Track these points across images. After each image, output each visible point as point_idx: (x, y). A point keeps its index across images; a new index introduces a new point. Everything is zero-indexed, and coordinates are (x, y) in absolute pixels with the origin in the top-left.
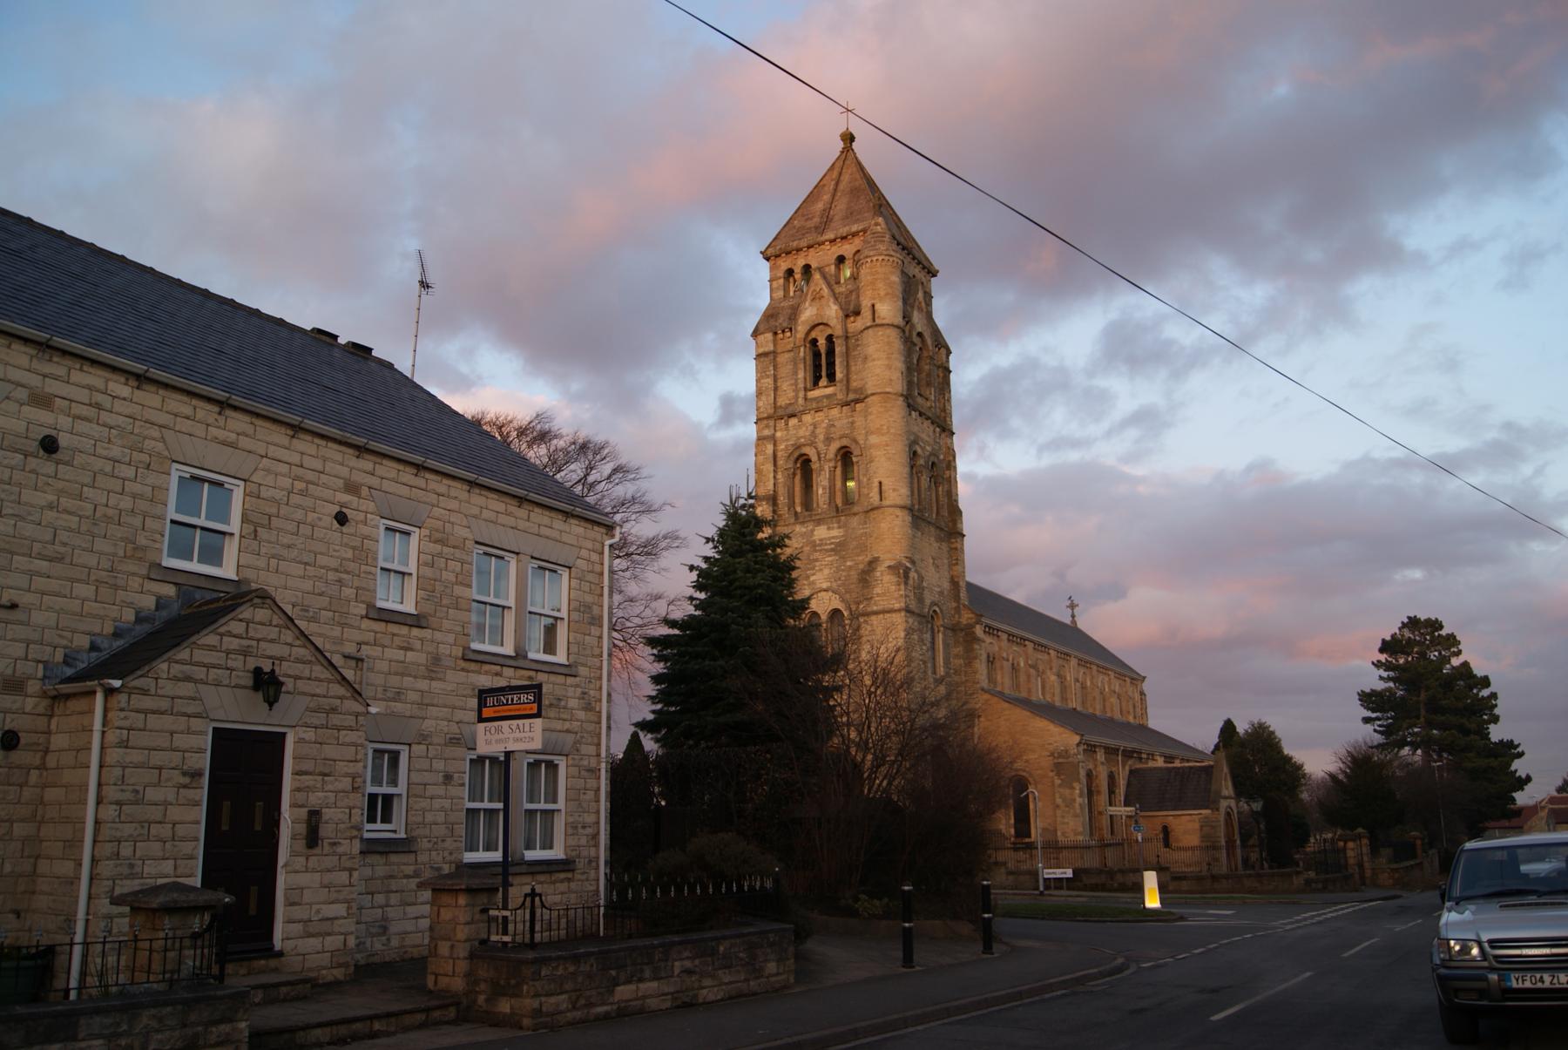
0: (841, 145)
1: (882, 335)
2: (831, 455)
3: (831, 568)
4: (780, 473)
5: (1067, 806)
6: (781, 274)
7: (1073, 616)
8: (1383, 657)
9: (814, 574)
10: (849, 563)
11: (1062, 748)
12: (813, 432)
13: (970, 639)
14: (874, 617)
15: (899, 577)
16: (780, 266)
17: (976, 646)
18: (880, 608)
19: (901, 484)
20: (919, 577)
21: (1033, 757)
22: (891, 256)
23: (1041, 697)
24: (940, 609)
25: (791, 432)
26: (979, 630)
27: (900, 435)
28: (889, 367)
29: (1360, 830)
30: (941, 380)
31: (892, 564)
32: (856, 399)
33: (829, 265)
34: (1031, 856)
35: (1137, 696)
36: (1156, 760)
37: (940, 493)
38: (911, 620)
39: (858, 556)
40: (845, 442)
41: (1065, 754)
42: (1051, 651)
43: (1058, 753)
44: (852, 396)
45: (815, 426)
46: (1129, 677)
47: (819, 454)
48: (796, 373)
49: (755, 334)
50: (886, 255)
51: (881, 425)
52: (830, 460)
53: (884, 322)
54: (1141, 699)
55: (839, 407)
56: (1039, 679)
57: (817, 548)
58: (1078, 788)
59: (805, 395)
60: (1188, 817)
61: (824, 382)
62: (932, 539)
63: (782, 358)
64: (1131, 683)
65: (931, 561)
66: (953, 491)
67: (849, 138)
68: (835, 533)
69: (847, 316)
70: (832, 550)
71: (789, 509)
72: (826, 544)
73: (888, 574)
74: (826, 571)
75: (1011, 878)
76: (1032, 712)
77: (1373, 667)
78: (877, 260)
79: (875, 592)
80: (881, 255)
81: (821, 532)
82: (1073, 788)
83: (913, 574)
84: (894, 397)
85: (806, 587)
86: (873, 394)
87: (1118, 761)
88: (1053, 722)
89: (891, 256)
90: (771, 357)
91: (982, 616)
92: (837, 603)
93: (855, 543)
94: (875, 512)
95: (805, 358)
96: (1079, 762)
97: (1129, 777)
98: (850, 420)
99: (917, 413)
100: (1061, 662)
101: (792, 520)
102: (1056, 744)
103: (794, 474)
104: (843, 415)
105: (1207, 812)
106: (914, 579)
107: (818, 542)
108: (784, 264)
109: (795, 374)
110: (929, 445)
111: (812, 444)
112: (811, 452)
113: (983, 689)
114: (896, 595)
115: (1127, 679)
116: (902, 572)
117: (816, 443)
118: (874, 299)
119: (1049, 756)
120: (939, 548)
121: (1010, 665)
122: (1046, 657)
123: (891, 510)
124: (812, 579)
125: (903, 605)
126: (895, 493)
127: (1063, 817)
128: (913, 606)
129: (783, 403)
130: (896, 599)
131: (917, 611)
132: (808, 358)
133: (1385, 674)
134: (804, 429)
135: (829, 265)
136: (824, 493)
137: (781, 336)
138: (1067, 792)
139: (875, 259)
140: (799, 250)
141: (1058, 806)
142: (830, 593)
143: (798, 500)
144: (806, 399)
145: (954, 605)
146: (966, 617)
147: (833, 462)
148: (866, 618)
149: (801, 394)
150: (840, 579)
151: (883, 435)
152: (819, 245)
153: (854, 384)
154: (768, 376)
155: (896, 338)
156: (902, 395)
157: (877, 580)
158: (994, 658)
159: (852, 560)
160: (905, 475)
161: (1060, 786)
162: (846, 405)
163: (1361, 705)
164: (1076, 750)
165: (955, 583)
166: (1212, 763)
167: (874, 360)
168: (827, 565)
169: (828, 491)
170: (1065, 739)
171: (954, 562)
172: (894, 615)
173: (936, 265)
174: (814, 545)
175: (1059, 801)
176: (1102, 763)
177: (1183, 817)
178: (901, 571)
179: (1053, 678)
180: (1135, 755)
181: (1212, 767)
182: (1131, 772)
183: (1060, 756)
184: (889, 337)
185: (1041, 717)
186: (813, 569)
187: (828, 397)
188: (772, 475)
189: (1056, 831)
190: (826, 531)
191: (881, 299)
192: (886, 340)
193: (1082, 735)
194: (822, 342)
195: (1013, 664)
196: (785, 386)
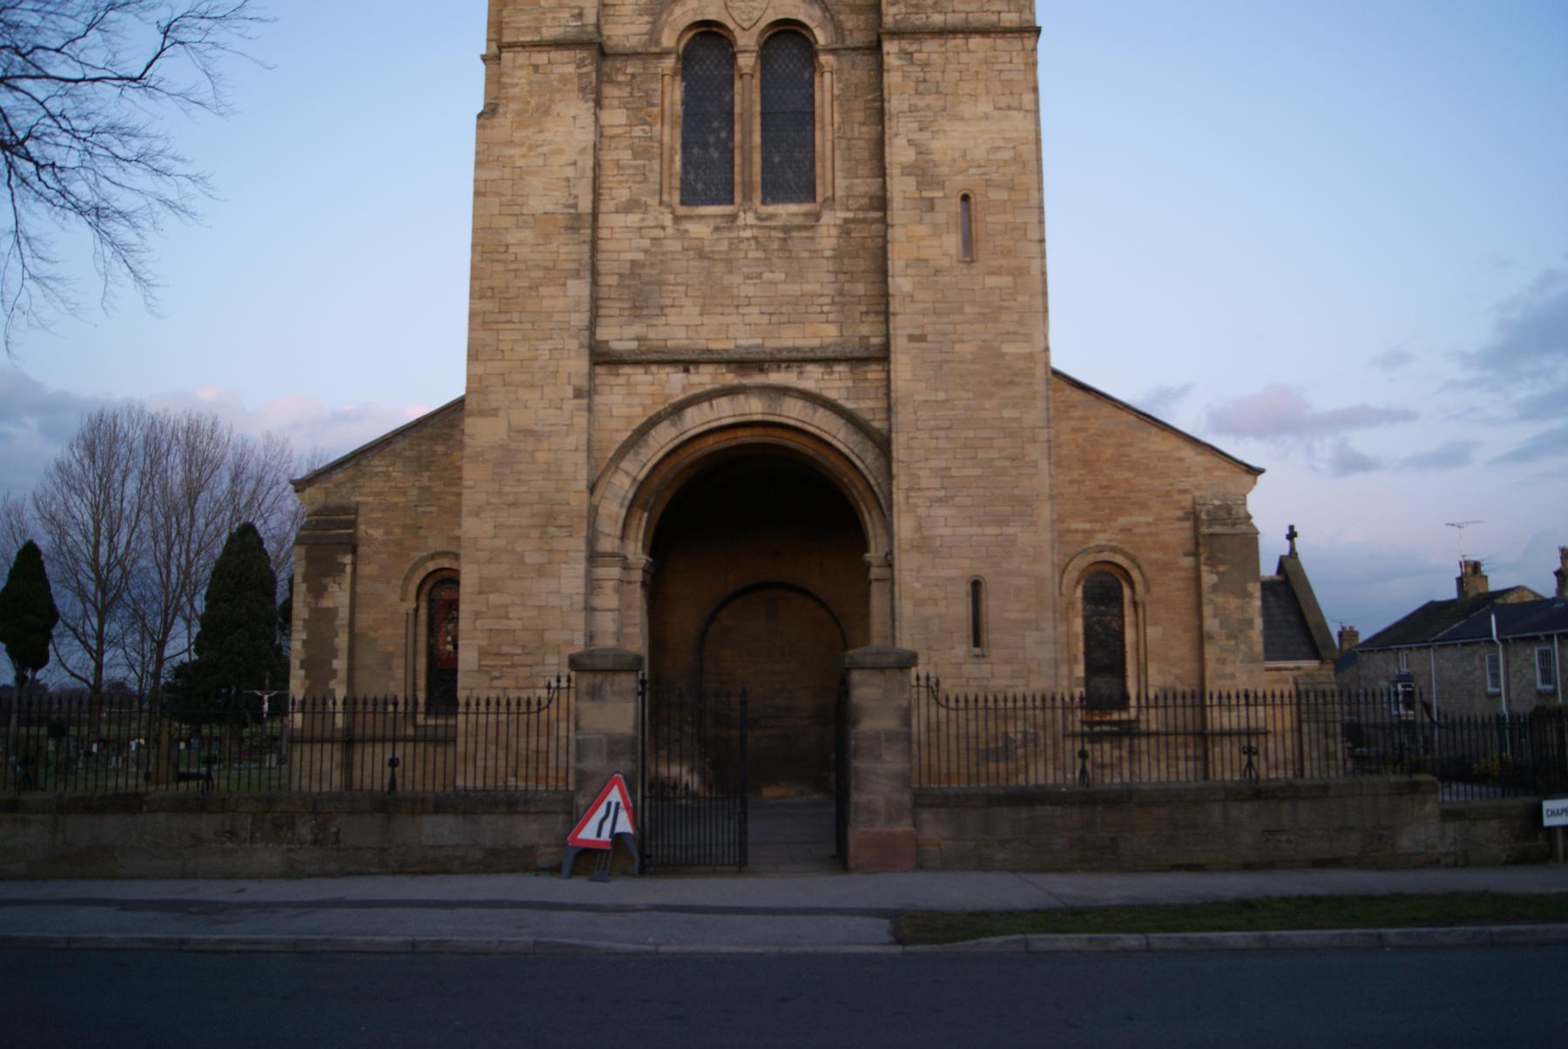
5: (1231, 636)
11: (1217, 503)
14: (932, 46)
18: (954, 19)
21: (1143, 519)
34: (1131, 752)
43: (1208, 512)
75: (1451, 829)
82: (1247, 595)
119: (1180, 519)
127: (1222, 661)
138: (1233, 602)
172: (1000, 43)
183: (1214, 520)
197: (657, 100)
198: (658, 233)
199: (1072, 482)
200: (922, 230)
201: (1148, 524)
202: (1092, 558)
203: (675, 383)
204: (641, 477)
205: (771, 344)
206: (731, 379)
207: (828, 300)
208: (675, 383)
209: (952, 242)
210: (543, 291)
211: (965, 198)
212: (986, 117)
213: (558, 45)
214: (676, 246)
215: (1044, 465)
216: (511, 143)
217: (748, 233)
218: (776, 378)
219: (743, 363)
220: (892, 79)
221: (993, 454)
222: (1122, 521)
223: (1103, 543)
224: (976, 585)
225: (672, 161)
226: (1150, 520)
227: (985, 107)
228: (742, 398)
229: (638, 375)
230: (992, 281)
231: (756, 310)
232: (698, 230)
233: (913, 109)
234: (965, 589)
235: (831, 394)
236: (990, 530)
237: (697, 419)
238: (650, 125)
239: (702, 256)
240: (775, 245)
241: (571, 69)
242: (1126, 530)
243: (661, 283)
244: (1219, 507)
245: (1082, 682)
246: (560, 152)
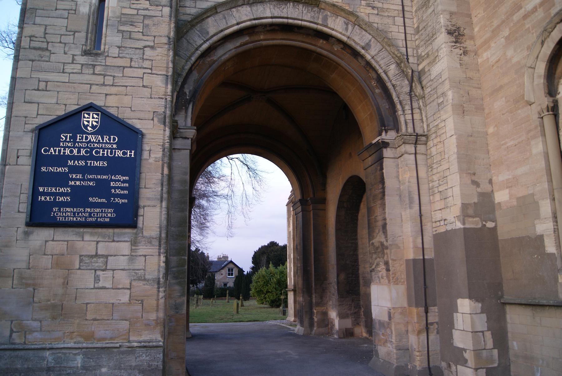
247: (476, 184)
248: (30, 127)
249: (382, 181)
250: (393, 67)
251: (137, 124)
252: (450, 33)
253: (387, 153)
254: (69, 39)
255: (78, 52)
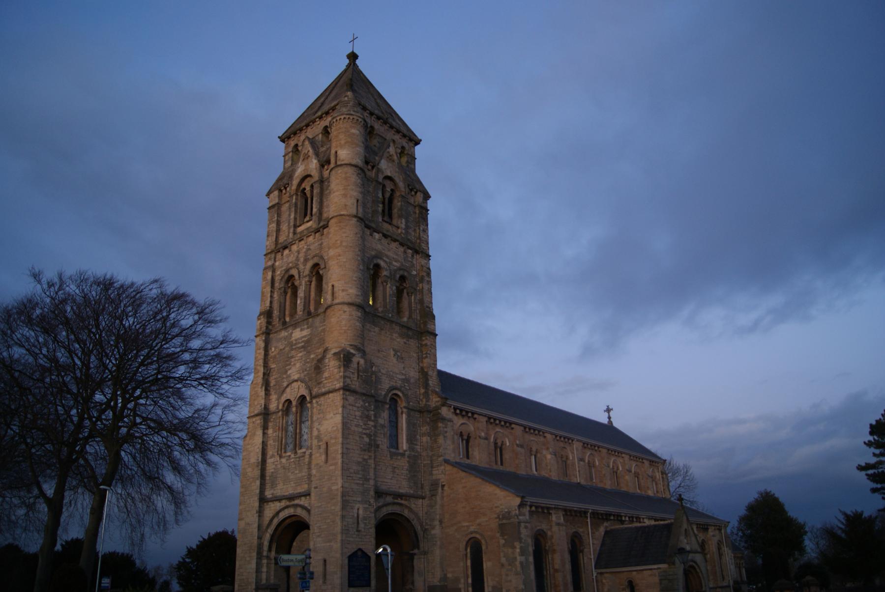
0: (347, 61)
1: (341, 173)
2: (307, 272)
3: (301, 362)
4: (276, 293)
5: (510, 565)
6: (290, 149)
7: (609, 418)
8: (871, 438)
9: (289, 369)
10: (312, 356)
11: (506, 510)
12: (297, 257)
13: (435, 417)
14: (322, 399)
15: (340, 361)
16: (291, 144)
17: (440, 425)
18: (327, 389)
19: (350, 286)
20: (366, 362)
22: (351, 115)
23: (535, 472)
24: (403, 393)
25: (284, 260)
26: (445, 412)
27: (351, 247)
28: (345, 196)
29: (809, 578)
30: (417, 216)
31: (337, 351)
32: (321, 228)
33: (318, 135)
35: (658, 475)
36: (644, 523)
37: (413, 301)
38: (351, 399)
39: (319, 349)
40: (316, 260)
41: (507, 515)
42: (546, 435)
44: (321, 224)
45: (298, 252)
46: (647, 460)
47: (299, 273)
48: (290, 215)
49: (268, 195)
50: (347, 114)
51: (336, 241)
52: (306, 276)
53: (343, 163)
54: (663, 478)
55: (313, 234)
56: (533, 457)
57: (294, 347)
58: (518, 547)
59: (294, 230)
60: (649, 572)
61: (307, 218)
62: (395, 335)
63: (285, 208)
64: (650, 465)
65: (392, 353)
66: (426, 299)
67: (353, 57)
68: (305, 333)
69: (322, 166)
70: (303, 347)
71: (280, 320)
72: (299, 343)
73: (333, 360)
74: (298, 365)
76: (483, 479)
77: (865, 446)
78: (340, 119)
79: (324, 377)
80: (342, 115)
81: (298, 334)
82: (514, 547)
83: (357, 359)
84: (348, 218)
85: (285, 380)
86: (332, 218)
87: (587, 522)
88: (498, 486)
89: (351, 115)
90: (276, 208)
91: (446, 399)
92: (304, 391)
93: (317, 339)
94: (329, 310)
95: (296, 204)
96: (519, 523)
97: (604, 537)
98: (320, 242)
99: (381, 235)
100: (562, 445)
101: (281, 327)
102: (501, 507)
103: (285, 293)
104: (316, 239)
105: (664, 566)
106: (358, 363)
107: (294, 342)
108: (292, 143)
109: (288, 215)
110: (396, 261)
111: (296, 266)
112: (294, 272)
113: (447, 461)
114: (337, 376)
115: (644, 461)
116: (346, 359)
117: (298, 265)
118: (336, 147)
120: (405, 343)
121: (492, 445)
122: (542, 439)
123: (340, 306)
124: (289, 372)
125: (342, 384)
126: (344, 293)
127: (507, 575)
128: (356, 385)
129: (283, 241)
130: (337, 380)
131: (358, 389)
132: (299, 203)
133: (877, 451)
134: (292, 256)
135: (318, 135)
136: (301, 303)
137: (284, 191)
138: (510, 550)
139: (338, 118)
140: (301, 130)
141: (503, 565)
142: (299, 383)
143: (287, 313)
144: (295, 233)
145: (423, 391)
146: (434, 401)
147: (308, 277)
148: (318, 400)
149: (292, 230)
150: (306, 370)
151: (337, 248)
152: (313, 123)
153: (325, 215)
154: (273, 222)
155: (353, 174)
156: (356, 216)
157: (326, 366)
158: (469, 437)
159: (314, 353)
160: (355, 279)
161: (504, 545)
162: (318, 232)
163: (868, 479)
164: (517, 512)
165: (424, 374)
166: (673, 521)
167: (334, 192)
168: (299, 360)
169: (303, 300)
170: (508, 500)
171: (424, 356)
172: (335, 394)
173: (419, 133)
174: (291, 345)
175: (503, 560)
176: (558, 524)
177: (645, 572)
178: (342, 356)
179: (549, 456)
180: (612, 518)
181: (671, 524)
182: (607, 533)
184: (346, 173)
185: (490, 483)
186: (290, 364)
187: (307, 229)
188: (269, 295)
189: (502, 588)
190: (300, 333)
191: (341, 147)
192: (344, 176)
193: (523, 497)
194: (308, 188)
195: (496, 444)
196: (284, 227)
197: (278, 425)
198: (276, 463)
199: (463, 507)
200: (318, 455)
201: (487, 521)
202: (469, 536)
203: (278, 505)
204: (272, 533)
205: (296, 492)
206: (288, 503)
207: (306, 477)
208: (278, 505)
209: (323, 457)
210: (253, 484)
211: (327, 443)
212: (332, 418)
213: (257, 415)
214: (279, 466)
215: (339, 523)
216: (248, 444)
217: (292, 460)
218: (296, 502)
219: (291, 498)
220: (315, 410)
221: (329, 521)
222: (478, 521)
223: (473, 530)
224: (325, 561)
225: (282, 441)
226: (487, 519)
227: (332, 415)
228: (289, 509)
229: (271, 505)
230: (331, 468)
231: (292, 482)
232: (284, 460)
233: (318, 419)
234: (322, 563)
235: (306, 505)
236: (328, 544)
237: (282, 515)
238: (275, 432)
239: (284, 468)
240: (297, 463)
241: (259, 422)
242: (479, 524)
243: (276, 478)
244: (506, 512)
245: (471, 585)
246: (256, 445)
247: (443, 571)
248: (347, 556)
249: (413, 567)
250: (419, 527)
251: (369, 554)
252: (439, 521)
253: (416, 557)
254: (353, 526)
255: (355, 530)
